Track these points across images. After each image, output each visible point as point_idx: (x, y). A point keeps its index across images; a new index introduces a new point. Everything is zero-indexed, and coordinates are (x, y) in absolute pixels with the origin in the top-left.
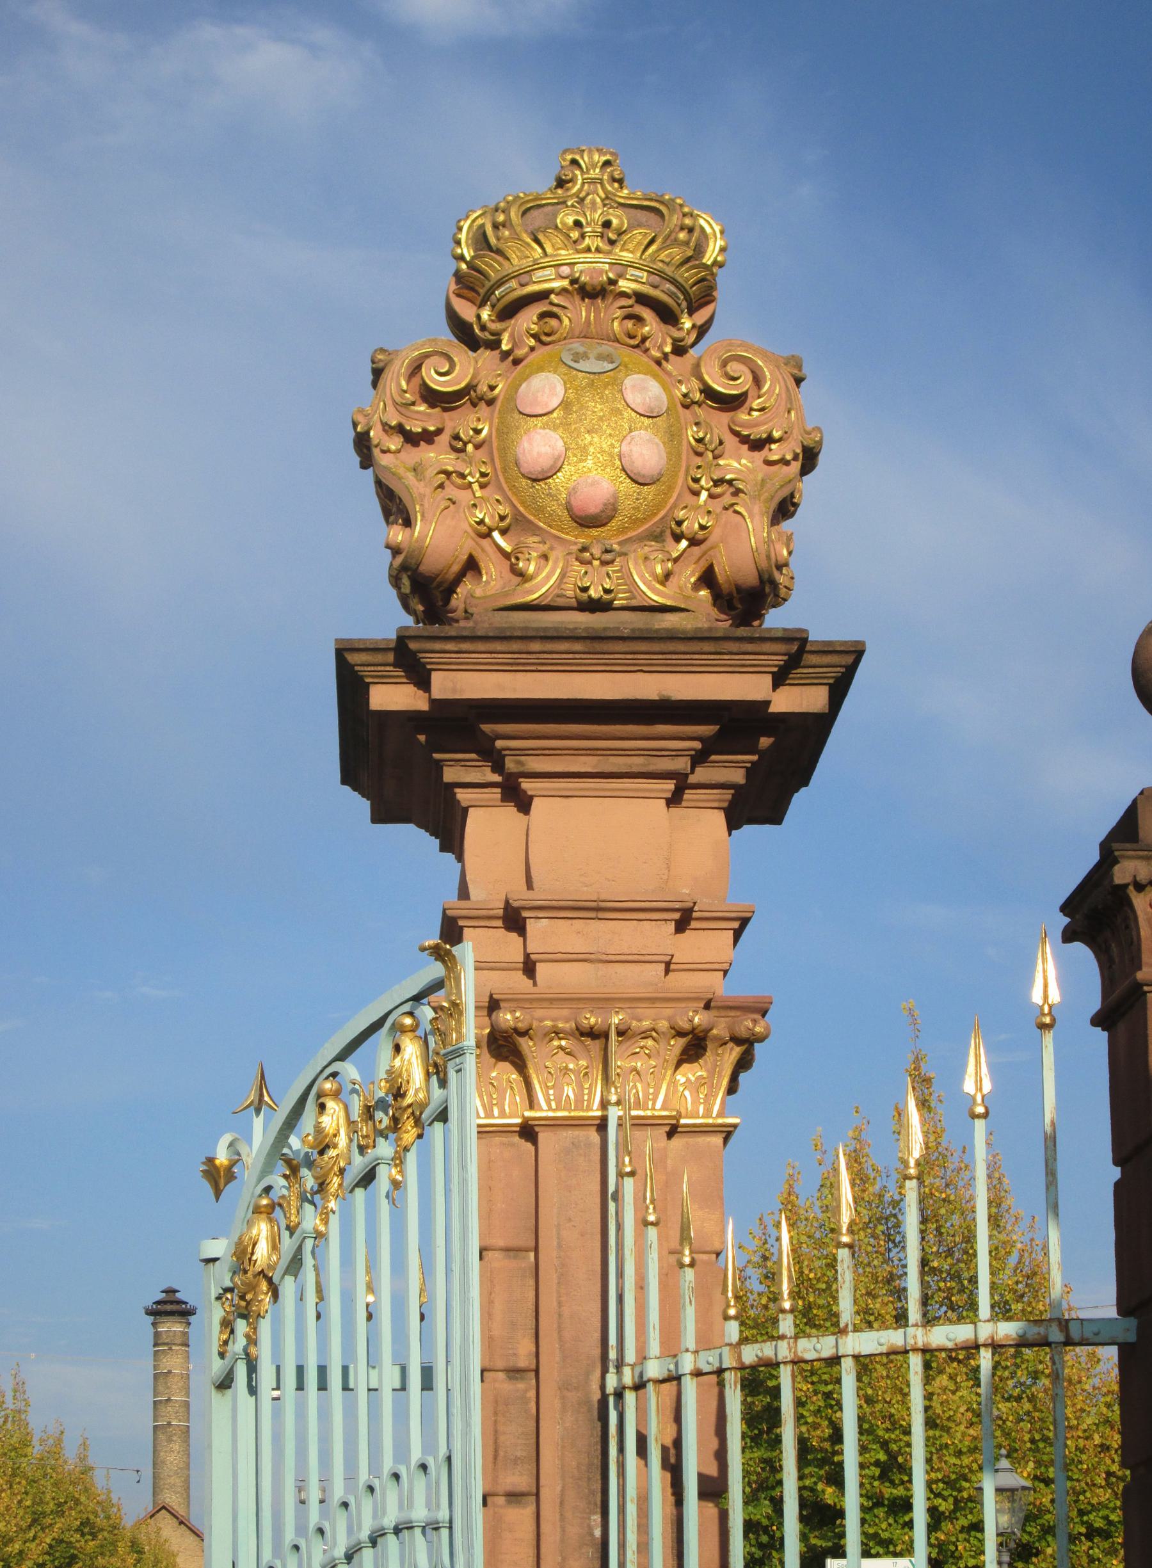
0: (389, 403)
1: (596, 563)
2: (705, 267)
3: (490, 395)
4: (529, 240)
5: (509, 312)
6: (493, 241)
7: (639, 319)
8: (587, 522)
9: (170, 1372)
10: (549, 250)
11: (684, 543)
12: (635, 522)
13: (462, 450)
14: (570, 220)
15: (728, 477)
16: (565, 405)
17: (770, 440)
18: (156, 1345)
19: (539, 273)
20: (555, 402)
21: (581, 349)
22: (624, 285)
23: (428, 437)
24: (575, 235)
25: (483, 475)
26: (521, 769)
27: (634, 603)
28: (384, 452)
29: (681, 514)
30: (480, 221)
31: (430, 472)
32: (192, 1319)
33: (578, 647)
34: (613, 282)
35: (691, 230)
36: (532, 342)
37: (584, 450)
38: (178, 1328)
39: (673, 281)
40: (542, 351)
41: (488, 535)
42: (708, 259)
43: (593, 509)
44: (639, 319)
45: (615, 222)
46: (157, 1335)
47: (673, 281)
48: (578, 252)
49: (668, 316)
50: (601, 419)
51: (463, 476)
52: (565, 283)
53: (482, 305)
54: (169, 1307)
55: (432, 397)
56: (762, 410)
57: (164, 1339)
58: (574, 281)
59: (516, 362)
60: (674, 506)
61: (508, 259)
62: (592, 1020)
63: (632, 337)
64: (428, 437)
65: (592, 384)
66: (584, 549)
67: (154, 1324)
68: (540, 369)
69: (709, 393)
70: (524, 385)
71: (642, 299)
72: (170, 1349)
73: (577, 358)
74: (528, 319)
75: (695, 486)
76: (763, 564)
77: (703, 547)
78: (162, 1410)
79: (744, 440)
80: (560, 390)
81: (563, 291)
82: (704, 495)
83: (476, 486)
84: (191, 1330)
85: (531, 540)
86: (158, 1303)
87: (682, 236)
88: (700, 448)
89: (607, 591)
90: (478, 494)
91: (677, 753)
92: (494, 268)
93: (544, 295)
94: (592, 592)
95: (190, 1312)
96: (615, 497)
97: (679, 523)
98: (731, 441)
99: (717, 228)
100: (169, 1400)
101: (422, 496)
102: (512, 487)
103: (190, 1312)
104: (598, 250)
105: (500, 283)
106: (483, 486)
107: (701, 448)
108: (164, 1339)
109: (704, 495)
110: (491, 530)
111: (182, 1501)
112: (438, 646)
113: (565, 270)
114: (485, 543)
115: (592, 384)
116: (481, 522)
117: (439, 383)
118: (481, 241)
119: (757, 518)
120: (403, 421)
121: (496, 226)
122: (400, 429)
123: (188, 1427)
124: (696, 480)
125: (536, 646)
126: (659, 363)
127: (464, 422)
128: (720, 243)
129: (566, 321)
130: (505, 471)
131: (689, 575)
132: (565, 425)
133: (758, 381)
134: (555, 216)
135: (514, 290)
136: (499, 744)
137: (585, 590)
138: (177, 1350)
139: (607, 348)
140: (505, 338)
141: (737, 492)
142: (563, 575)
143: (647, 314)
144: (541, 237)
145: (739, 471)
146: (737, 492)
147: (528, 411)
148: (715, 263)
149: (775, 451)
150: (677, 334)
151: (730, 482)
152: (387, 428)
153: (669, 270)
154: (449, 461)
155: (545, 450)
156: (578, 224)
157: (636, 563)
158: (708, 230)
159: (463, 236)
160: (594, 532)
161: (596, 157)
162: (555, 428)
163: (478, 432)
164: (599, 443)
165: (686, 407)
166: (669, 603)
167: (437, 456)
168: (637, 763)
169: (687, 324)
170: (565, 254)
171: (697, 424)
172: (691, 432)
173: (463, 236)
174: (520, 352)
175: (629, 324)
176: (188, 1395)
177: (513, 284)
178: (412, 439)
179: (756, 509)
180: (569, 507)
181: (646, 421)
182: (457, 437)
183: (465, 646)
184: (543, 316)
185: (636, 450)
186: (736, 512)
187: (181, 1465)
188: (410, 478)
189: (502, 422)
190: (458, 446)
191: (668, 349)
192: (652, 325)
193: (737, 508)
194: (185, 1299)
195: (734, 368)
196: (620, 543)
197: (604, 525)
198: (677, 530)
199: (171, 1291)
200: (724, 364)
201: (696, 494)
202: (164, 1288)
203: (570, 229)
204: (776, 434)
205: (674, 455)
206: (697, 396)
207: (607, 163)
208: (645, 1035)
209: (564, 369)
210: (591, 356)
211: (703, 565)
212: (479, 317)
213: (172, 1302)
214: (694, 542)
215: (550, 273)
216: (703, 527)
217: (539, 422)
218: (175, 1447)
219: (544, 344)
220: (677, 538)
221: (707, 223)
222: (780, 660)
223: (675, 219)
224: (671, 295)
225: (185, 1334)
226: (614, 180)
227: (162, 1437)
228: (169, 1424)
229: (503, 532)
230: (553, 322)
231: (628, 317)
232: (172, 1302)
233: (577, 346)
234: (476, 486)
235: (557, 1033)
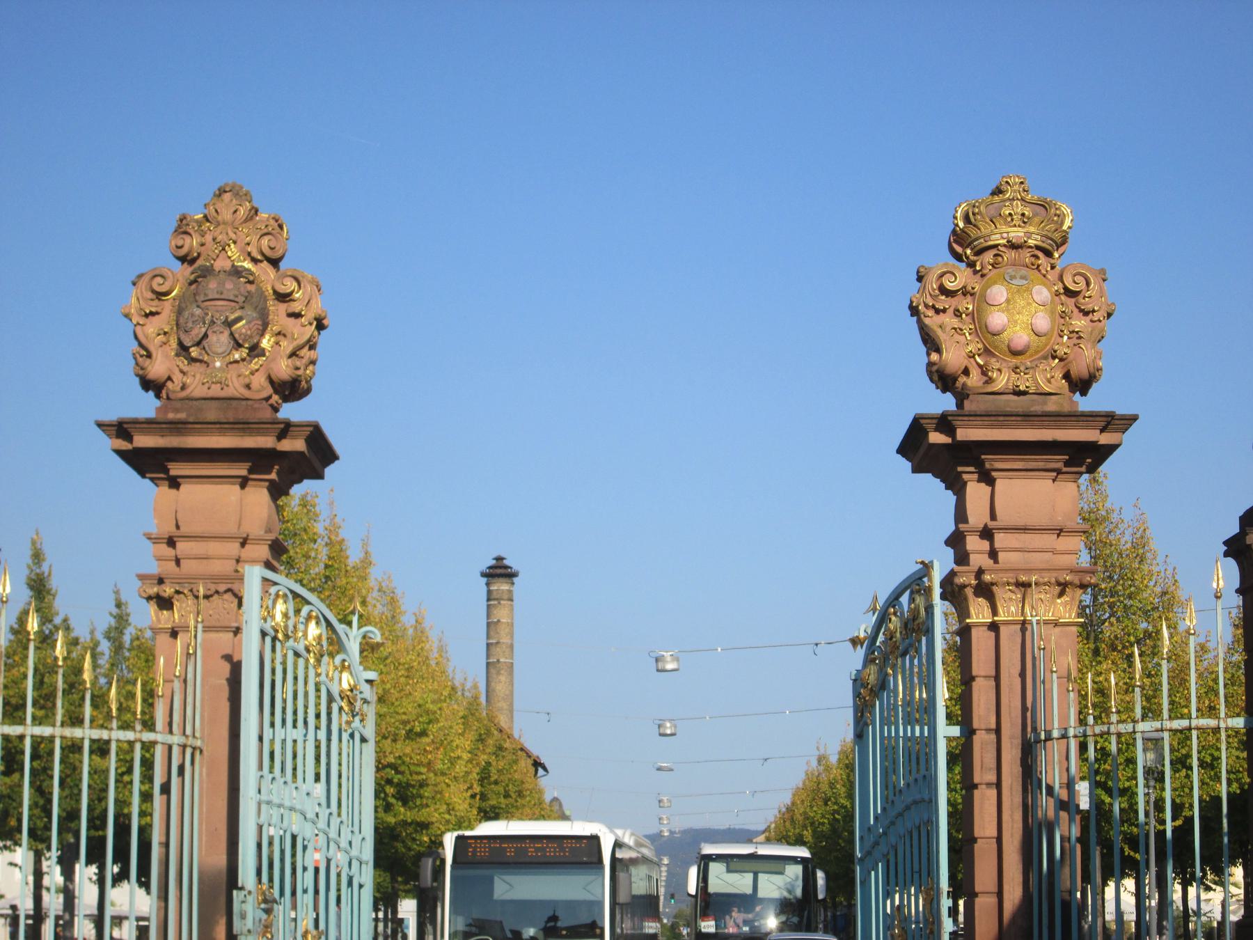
0: (928, 294)
1: (1022, 374)
2: (1065, 231)
3: (972, 291)
4: (988, 220)
5: (979, 252)
6: (973, 220)
7: (1037, 257)
8: (1015, 353)
9: (499, 621)
10: (998, 226)
11: (1057, 361)
12: (1037, 352)
13: (961, 316)
14: (1007, 212)
15: (1077, 330)
16: (1008, 301)
17: (1094, 311)
18: (488, 600)
19: (993, 236)
20: (1003, 299)
21: (1013, 274)
22: (1031, 242)
23: (944, 311)
24: (1009, 219)
25: (970, 329)
26: (992, 467)
27: (1038, 391)
28: (925, 316)
29: (1056, 347)
30: (966, 208)
31: (948, 329)
32: (515, 580)
33: (1019, 418)
34: (1025, 242)
35: (1059, 216)
36: (990, 267)
37: (1016, 322)
38: (505, 587)
39: (1052, 239)
40: (995, 271)
41: (973, 357)
42: (1065, 227)
43: (1019, 348)
44: (1037, 257)
45: (1027, 213)
46: (489, 592)
47: (1052, 239)
48: (1011, 227)
49: (1048, 254)
50: (1023, 308)
51: (961, 330)
52: (1004, 241)
53: (967, 247)
54: (499, 571)
55: (944, 291)
56: (1090, 297)
57: (495, 595)
58: (1008, 242)
59: (983, 276)
60: (1054, 343)
61: (979, 229)
62: (1023, 578)
63: (1033, 265)
64: (944, 311)
65: (1018, 291)
66: (1017, 368)
67: (488, 584)
68: (995, 283)
69: (1066, 288)
70: (989, 291)
71: (1038, 248)
72: (499, 603)
73: (1012, 278)
74: (988, 257)
75: (1062, 333)
76: (1092, 370)
77: (1066, 361)
78: (494, 650)
79: (1081, 311)
80: (1005, 294)
81: (1005, 246)
82: (1066, 337)
83: (967, 334)
84: (515, 589)
85: (994, 360)
86: (490, 568)
87: (1055, 218)
88: (1063, 315)
89: (1027, 387)
90: (969, 338)
91: (1058, 461)
92: (973, 233)
93: (995, 246)
94: (1021, 388)
95: (514, 575)
96: (1029, 342)
97: (1055, 351)
98: (1076, 310)
99: (1069, 211)
100: (498, 643)
101: (945, 340)
102: (984, 337)
103: (514, 575)
104: (1019, 226)
105: (976, 239)
106: (970, 334)
107: (1063, 315)
109: (1066, 337)
110: (974, 355)
111: (507, 720)
112: (960, 418)
113: (1005, 235)
114: (972, 360)
115: (1018, 291)
116: (971, 351)
117: (950, 286)
118: (967, 219)
119: (1089, 351)
120: (935, 303)
121: (974, 214)
122: (933, 307)
123: (512, 663)
124: (1062, 331)
125: (1001, 418)
126: (1044, 276)
128: (1071, 218)
129: (1005, 258)
130: (980, 328)
131: (1059, 374)
132: (1008, 310)
133: (1088, 284)
134: (1001, 209)
135: (981, 243)
136: (983, 457)
137: (1017, 386)
138: (504, 605)
139: (1024, 271)
140: (978, 264)
141: (1080, 338)
142: (1008, 379)
143: (1040, 254)
144: (994, 220)
145: (1081, 327)
146: (1080, 338)
147: (991, 303)
148: (1069, 228)
149: (1096, 316)
150: (1053, 261)
151: (1077, 332)
152: (926, 306)
153: (1049, 235)
154: (955, 322)
155: (999, 322)
156: (1010, 214)
157: (1039, 374)
158: (1065, 212)
159: (958, 215)
160: (1020, 357)
161: (1017, 180)
162: (1003, 312)
163: (967, 309)
164: (1023, 318)
165: (1057, 295)
166: (1053, 392)
167: (949, 320)
168: (1041, 465)
169: (1056, 255)
170: (1004, 229)
171: (1062, 304)
172: (1060, 308)
173: (958, 215)
174: (985, 272)
175: (1033, 259)
176: (512, 637)
177: (982, 240)
178: (937, 311)
179: (1089, 346)
180: (1009, 346)
181: (1042, 307)
182: (958, 311)
183: (971, 418)
184: (996, 255)
185: (1038, 321)
186: (1080, 347)
187: (507, 692)
188: (939, 332)
189: (978, 306)
190: (958, 313)
191: (1049, 269)
192: (1043, 260)
193: (1081, 345)
194: (511, 566)
195: (1078, 278)
196: (1031, 362)
197: (1023, 354)
198: (1054, 354)
199: (499, 559)
200: (1075, 275)
201: (1062, 337)
202: (495, 556)
203: (1007, 217)
204: (1096, 308)
205: (1053, 321)
206: (1062, 291)
207: (1022, 183)
208: (1045, 584)
209: (1006, 283)
210: (1018, 277)
211: (1065, 370)
212: (966, 253)
213: (500, 567)
214: (1061, 360)
215: (998, 236)
216: (1065, 354)
217: (996, 308)
218: (503, 678)
219: (995, 268)
220: (1054, 358)
221: (1066, 209)
222: (1103, 424)
223: (1053, 211)
224: (1050, 245)
225: (510, 592)
226: (1024, 191)
227: (493, 671)
228: (498, 661)
229: (979, 355)
230: (1000, 259)
231: (1033, 256)
232: (500, 567)
233: (1011, 270)
234: (967, 334)
235: (1008, 584)
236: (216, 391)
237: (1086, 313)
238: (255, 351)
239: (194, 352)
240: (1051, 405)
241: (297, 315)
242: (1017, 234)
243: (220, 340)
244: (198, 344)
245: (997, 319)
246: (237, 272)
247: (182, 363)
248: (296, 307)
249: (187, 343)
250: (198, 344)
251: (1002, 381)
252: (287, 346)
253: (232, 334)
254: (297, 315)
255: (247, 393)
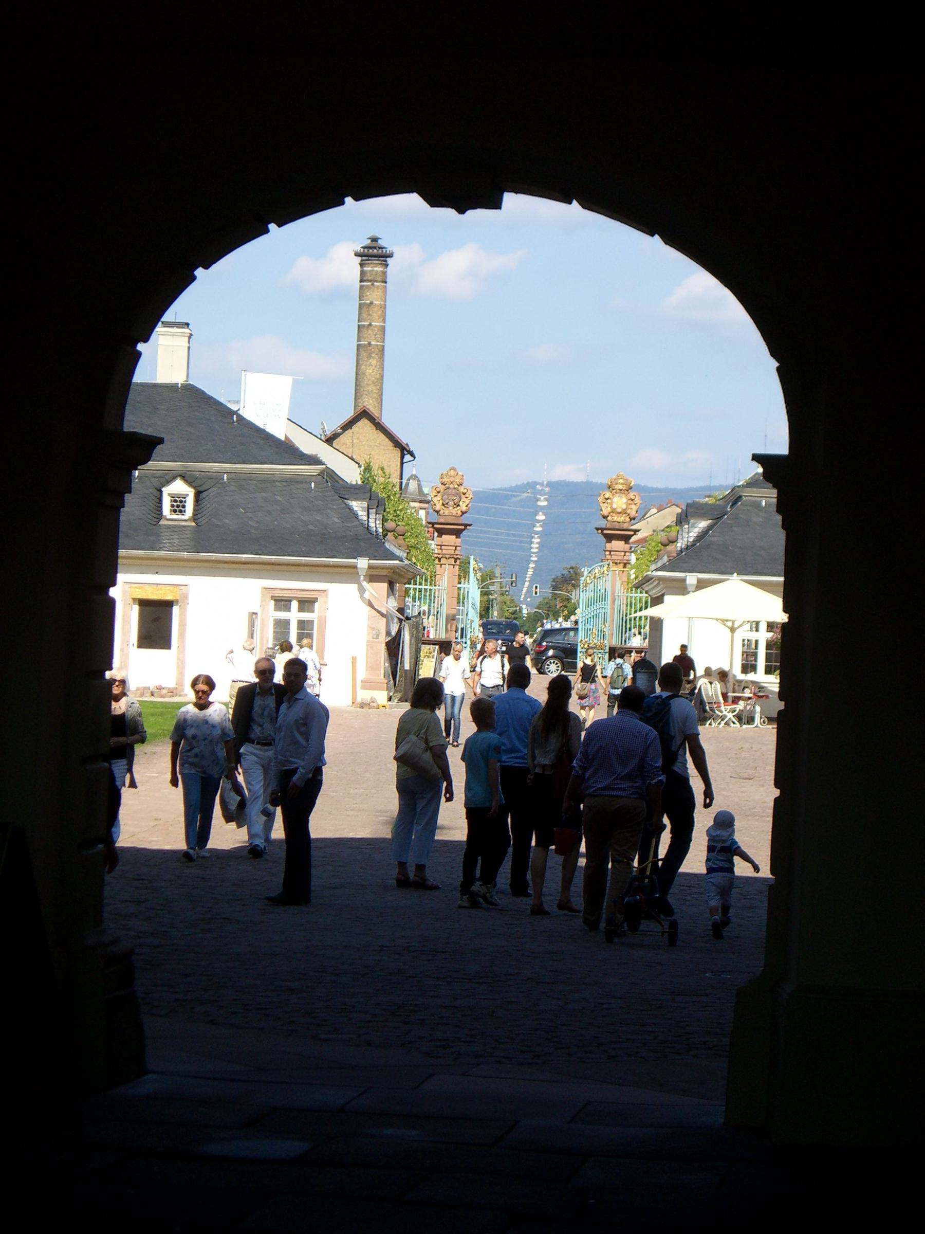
5: (613, 490)
8: (620, 513)
18: (361, 281)
22: (624, 488)
38: (379, 269)
46: (363, 273)
49: (627, 491)
55: (605, 498)
57: (368, 277)
62: (616, 561)
67: (362, 265)
72: (373, 285)
74: (614, 491)
108: (368, 277)
118: (611, 483)
127: (609, 501)
133: (635, 496)
135: (614, 488)
139: (622, 495)
178: (604, 503)
195: (634, 496)
236: (451, 515)
237: (635, 504)
238: (458, 506)
239: (446, 505)
240: (625, 526)
241: (467, 498)
242: (621, 487)
243: (451, 503)
244: (447, 504)
245: (615, 506)
246: (455, 488)
247: (443, 507)
248: (467, 495)
249: (444, 503)
250: (447, 504)
251: (616, 518)
252: (465, 505)
253: (454, 502)
254: (467, 498)
255: (457, 515)
